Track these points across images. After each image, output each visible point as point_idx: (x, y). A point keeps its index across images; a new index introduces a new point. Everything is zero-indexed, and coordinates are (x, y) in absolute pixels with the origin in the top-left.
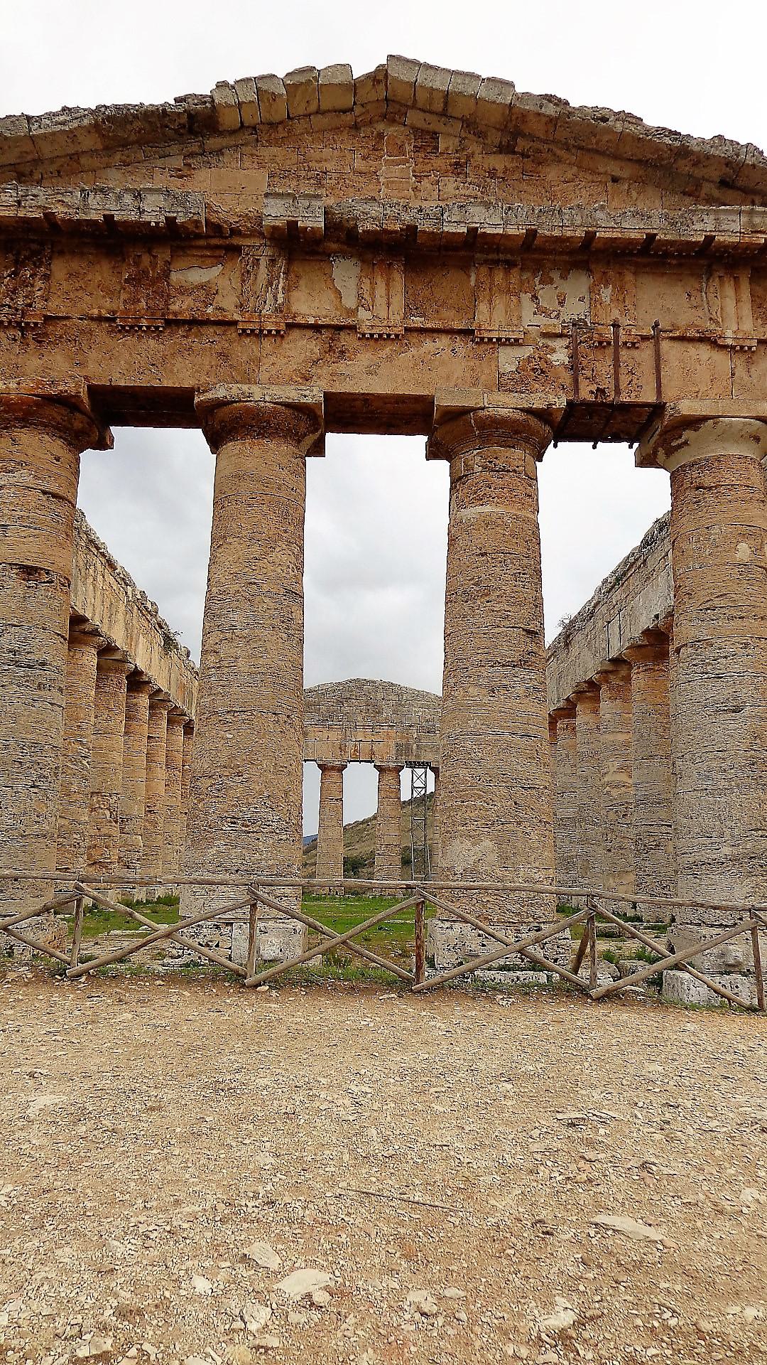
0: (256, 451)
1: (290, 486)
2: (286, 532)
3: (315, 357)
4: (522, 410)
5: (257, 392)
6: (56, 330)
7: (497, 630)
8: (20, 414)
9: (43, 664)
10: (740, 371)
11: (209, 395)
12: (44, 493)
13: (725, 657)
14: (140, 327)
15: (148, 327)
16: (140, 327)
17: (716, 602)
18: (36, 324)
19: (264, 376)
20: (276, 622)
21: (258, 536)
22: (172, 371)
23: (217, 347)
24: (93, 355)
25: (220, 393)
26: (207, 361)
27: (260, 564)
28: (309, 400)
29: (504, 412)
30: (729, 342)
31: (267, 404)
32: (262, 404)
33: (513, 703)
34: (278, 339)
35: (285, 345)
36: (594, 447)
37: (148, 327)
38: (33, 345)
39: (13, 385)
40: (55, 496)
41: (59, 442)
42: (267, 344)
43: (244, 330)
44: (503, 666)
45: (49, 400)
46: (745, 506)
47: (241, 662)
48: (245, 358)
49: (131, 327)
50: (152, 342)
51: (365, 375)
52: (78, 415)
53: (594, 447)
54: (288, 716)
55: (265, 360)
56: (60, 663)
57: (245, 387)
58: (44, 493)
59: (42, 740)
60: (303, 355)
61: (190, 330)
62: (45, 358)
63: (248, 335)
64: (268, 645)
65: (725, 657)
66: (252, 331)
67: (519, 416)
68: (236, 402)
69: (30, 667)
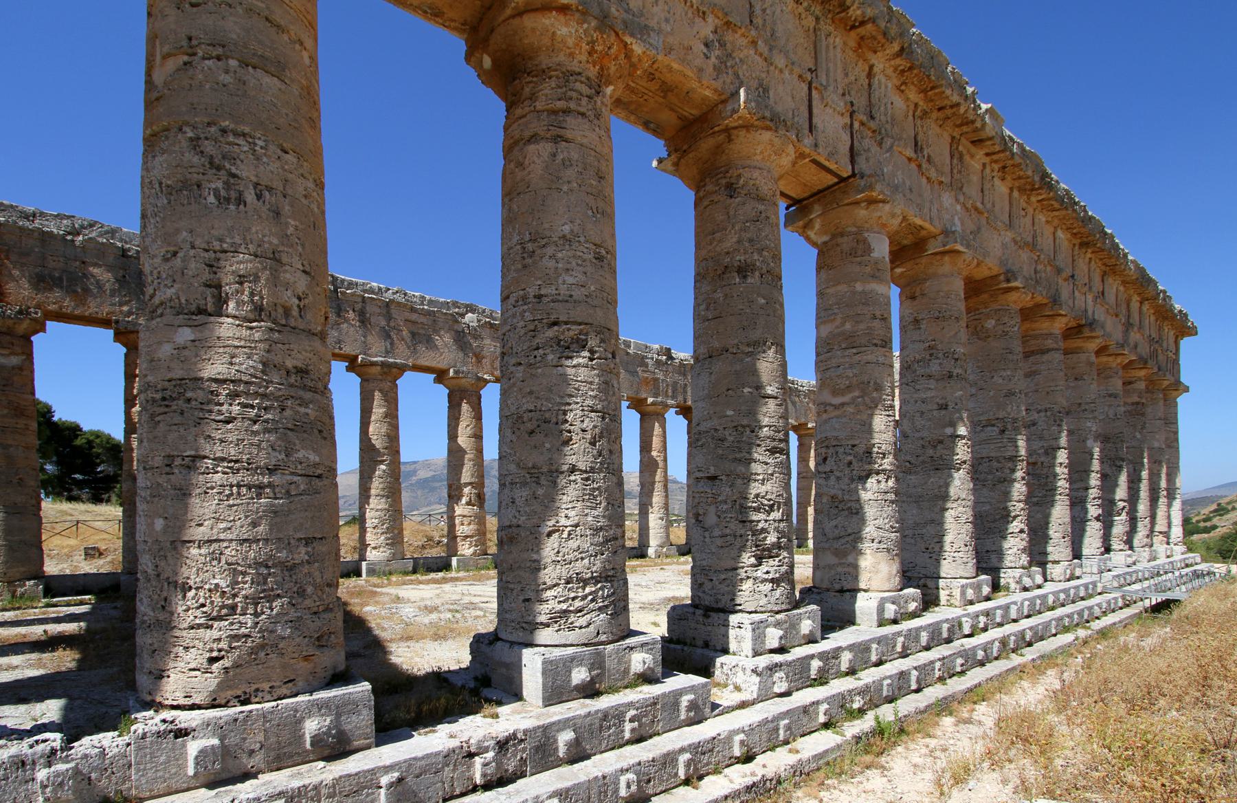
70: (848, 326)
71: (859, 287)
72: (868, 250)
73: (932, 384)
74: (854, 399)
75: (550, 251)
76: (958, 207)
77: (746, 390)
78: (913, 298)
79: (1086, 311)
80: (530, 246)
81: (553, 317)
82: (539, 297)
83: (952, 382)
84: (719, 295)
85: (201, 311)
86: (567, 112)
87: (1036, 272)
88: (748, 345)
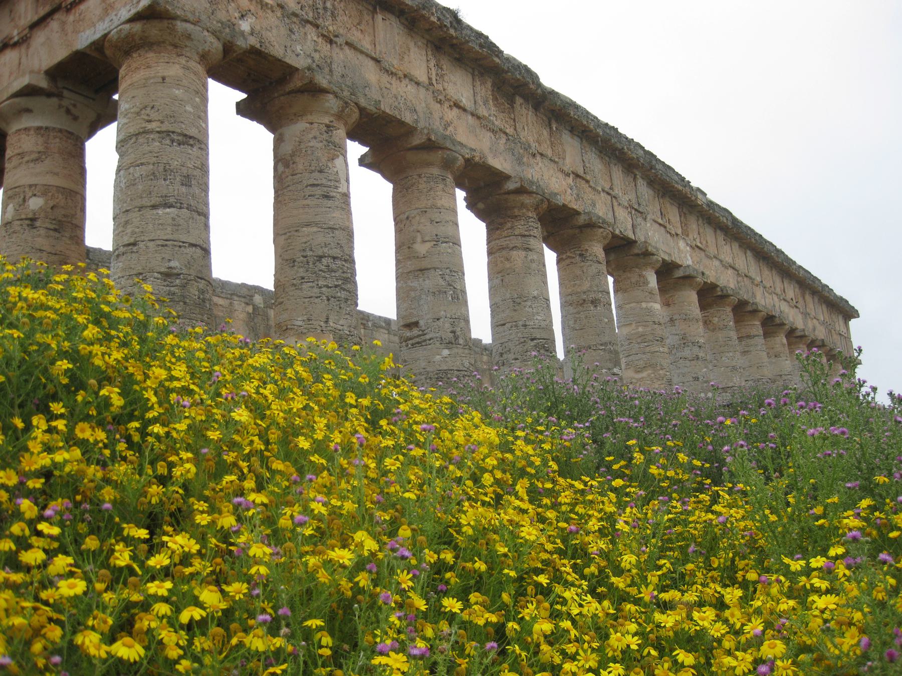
10: (24, 60)
30: (16, 39)
70: (640, 329)
71: (644, 305)
72: (646, 283)
73: (688, 363)
74: (649, 375)
75: (529, 303)
76: (688, 248)
77: (604, 371)
78: (668, 305)
79: (774, 306)
80: (518, 300)
81: (534, 336)
82: (525, 326)
83: (700, 363)
84: (582, 315)
85: (450, 343)
86: (530, 236)
87: (738, 282)
88: (601, 345)
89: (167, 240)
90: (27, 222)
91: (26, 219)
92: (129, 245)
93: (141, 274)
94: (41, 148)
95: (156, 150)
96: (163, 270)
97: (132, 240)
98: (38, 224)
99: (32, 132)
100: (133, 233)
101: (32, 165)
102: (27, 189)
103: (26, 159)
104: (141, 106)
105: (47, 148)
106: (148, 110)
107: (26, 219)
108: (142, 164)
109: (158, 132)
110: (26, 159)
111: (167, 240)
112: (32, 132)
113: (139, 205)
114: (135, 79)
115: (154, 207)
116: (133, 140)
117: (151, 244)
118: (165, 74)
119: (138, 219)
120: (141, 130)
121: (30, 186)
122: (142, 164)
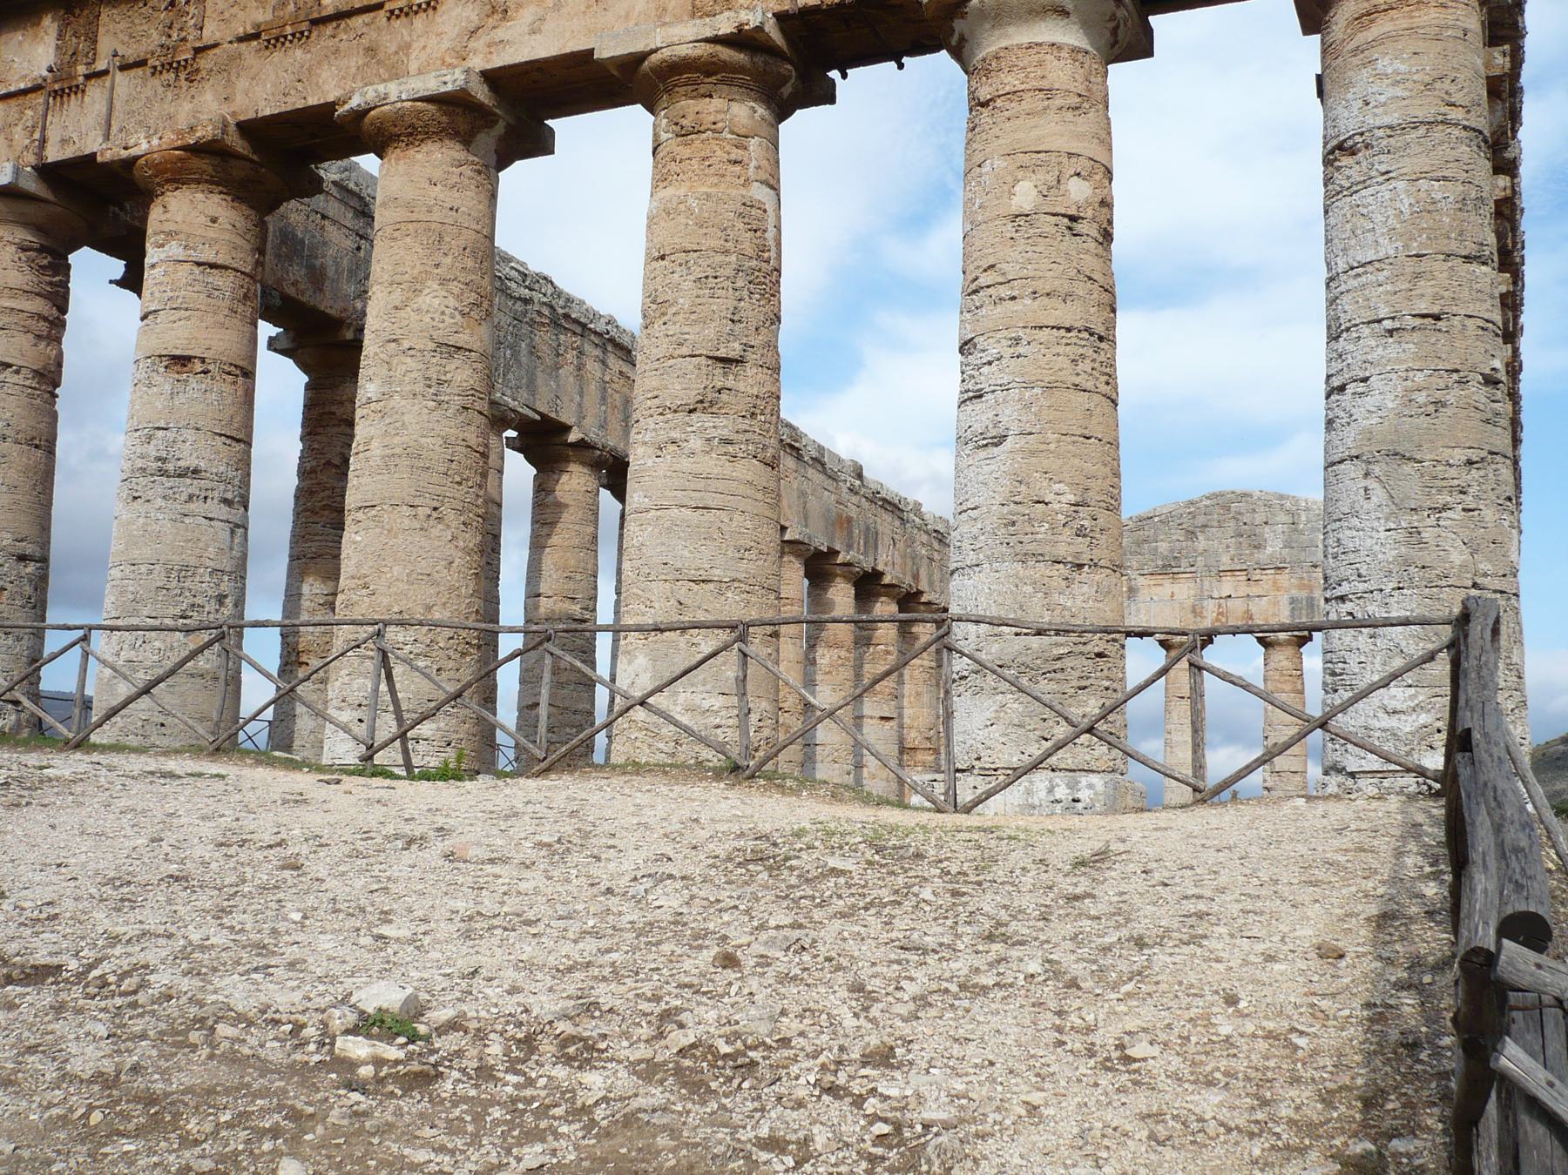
0: (402, 167)
1: (445, 205)
2: (437, 266)
3: (472, 27)
4: (707, 40)
5: (393, 90)
6: (205, 63)
7: (672, 362)
8: (168, 175)
9: (195, 471)
11: (347, 107)
12: (199, 264)
13: (990, 363)
14: (285, 37)
15: (293, 35)
16: (285, 37)
17: (983, 281)
18: (186, 60)
19: (413, 67)
20: (419, 388)
21: (398, 278)
22: (317, 84)
23: (365, 41)
24: (242, 84)
25: (355, 102)
26: (355, 61)
27: (402, 314)
28: (449, 88)
29: (684, 51)
31: (405, 104)
32: (399, 105)
33: (685, 464)
34: (430, 11)
35: (439, 20)
36: (901, 66)
37: (293, 35)
38: (184, 83)
39: (155, 142)
40: (213, 266)
41: (216, 198)
42: (419, 21)
43: (392, 12)
44: (675, 411)
45: (197, 149)
46: (1034, 121)
47: (375, 444)
48: (393, 49)
49: (277, 39)
50: (299, 53)
51: (527, 37)
52: (234, 162)
53: (901, 66)
54: (435, 509)
55: (415, 45)
56: (222, 469)
57: (381, 88)
58: (199, 264)
59: (193, 561)
60: (457, 28)
61: (338, 26)
62: (195, 101)
63: (398, 17)
64: (406, 418)
65: (990, 363)
66: (401, 10)
67: (703, 50)
68: (373, 108)
69: (180, 476)
89: (1487, 321)
90: (1066, 220)
91: (1064, 216)
92: (1424, 316)
93: (1457, 371)
94: (1081, 89)
95: (1465, 158)
96: (1487, 371)
97: (1435, 310)
98: (1079, 227)
99: (1064, 54)
100: (1436, 298)
101: (1069, 115)
102: (1065, 160)
103: (1058, 102)
104: (1435, 74)
105: (1089, 90)
106: (1447, 85)
107: (1064, 216)
108: (1445, 179)
109: (1465, 128)
110: (1058, 102)
111: (1487, 321)
112: (1064, 54)
113: (1446, 250)
114: (1417, 22)
115: (1468, 258)
116: (1422, 130)
117: (1469, 322)
118: (1468, 26)
119: (1445, 275)
120: (1440, 118)
121: (1070, 155)
122: (1445, 179)
